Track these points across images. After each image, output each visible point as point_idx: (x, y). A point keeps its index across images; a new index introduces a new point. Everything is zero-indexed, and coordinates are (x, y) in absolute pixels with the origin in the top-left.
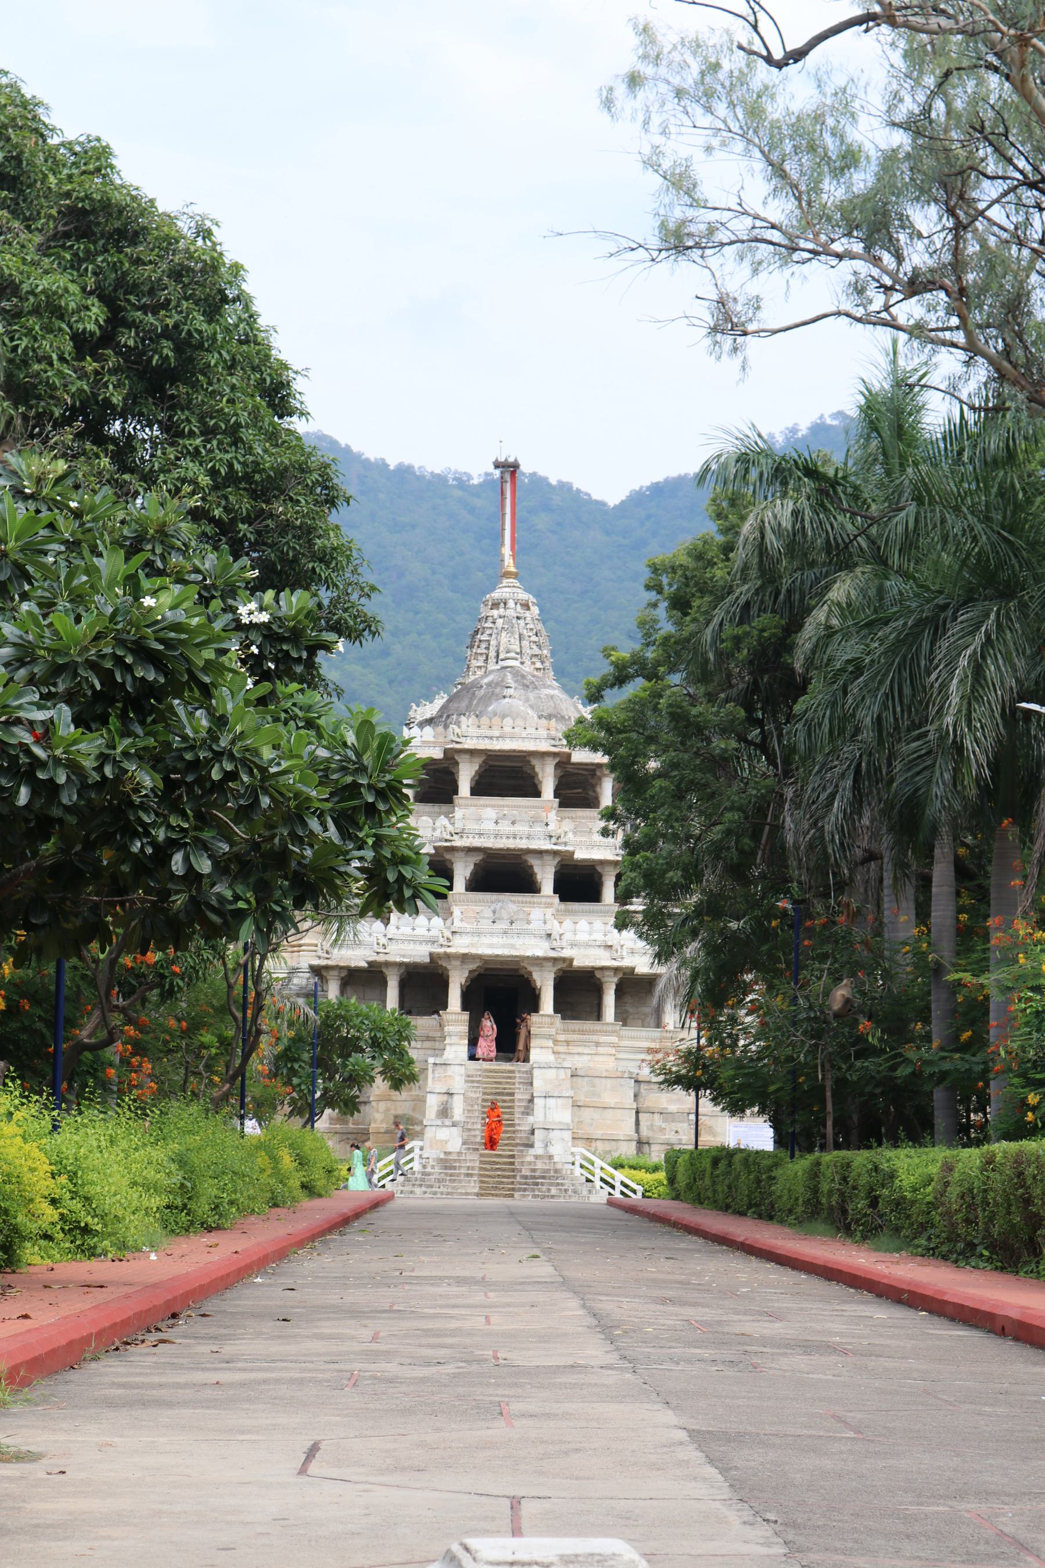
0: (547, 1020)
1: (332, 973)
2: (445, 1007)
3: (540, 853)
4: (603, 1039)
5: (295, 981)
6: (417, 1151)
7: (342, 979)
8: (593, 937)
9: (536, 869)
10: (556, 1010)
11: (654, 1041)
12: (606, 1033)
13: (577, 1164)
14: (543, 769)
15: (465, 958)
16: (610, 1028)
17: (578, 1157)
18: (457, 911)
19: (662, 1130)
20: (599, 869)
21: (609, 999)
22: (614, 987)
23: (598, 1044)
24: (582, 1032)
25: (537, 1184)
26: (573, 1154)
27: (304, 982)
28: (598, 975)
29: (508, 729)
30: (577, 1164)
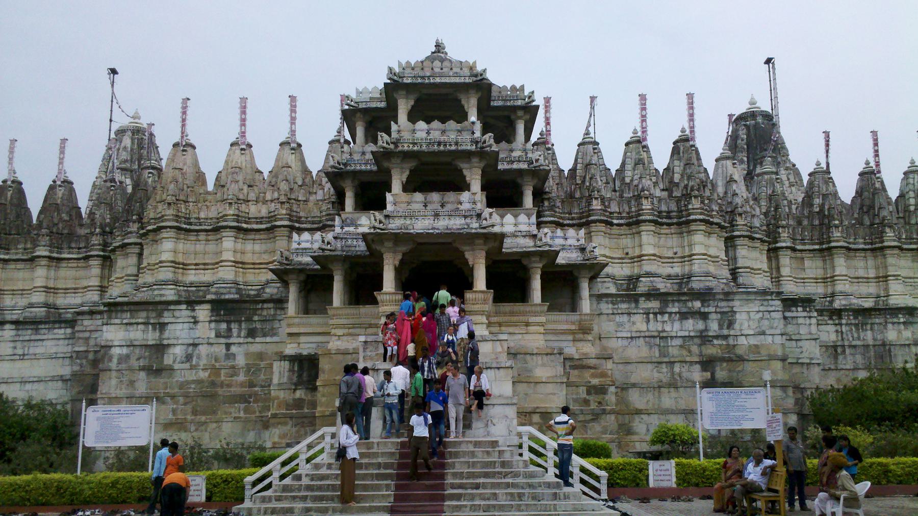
0: (481, 296)
1: (291, 276)
2: (380, 287)
3: (467, 155)
4: (532, 319)
5: (268, 290)
6: (328, 439)
7: (300, 282)
8: (518, 229)
9: (465, 172)
10: (489, 285)
11: (573, 323)
12: (536, 314)
13: (525, 447)
14: (468, 102)
15: (398, 238)
16: (538, 309)
17: (525, 439)
18: (389, 197)
19: (586, 402)
20: (519, 181)
21: (536, 284)
22: (539, 272)
23: (527, 324)
24: (512, 314)
25: (477, 487)
26: (520, 435)
27: (275, 291)
28: (525, 262)
29: (437, 70)
30: (525, 447)
